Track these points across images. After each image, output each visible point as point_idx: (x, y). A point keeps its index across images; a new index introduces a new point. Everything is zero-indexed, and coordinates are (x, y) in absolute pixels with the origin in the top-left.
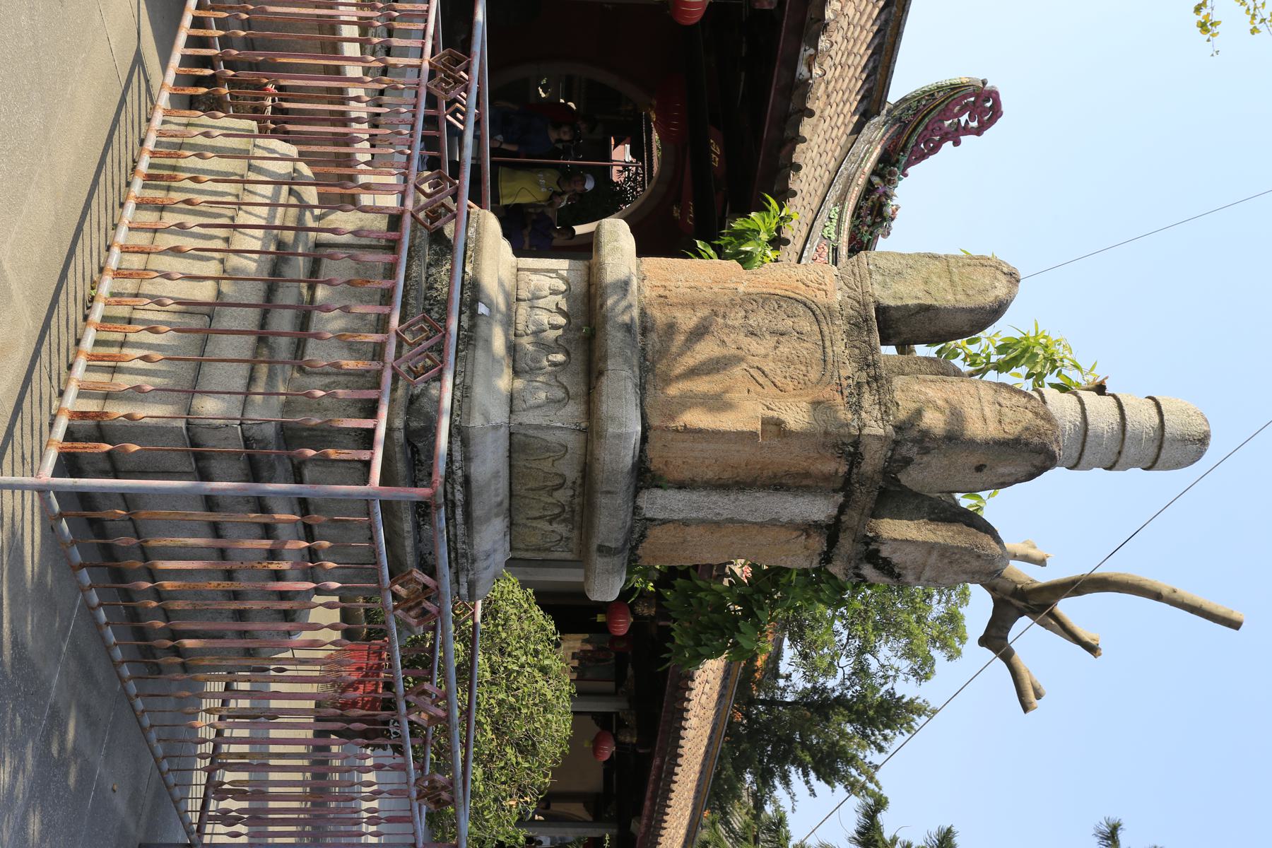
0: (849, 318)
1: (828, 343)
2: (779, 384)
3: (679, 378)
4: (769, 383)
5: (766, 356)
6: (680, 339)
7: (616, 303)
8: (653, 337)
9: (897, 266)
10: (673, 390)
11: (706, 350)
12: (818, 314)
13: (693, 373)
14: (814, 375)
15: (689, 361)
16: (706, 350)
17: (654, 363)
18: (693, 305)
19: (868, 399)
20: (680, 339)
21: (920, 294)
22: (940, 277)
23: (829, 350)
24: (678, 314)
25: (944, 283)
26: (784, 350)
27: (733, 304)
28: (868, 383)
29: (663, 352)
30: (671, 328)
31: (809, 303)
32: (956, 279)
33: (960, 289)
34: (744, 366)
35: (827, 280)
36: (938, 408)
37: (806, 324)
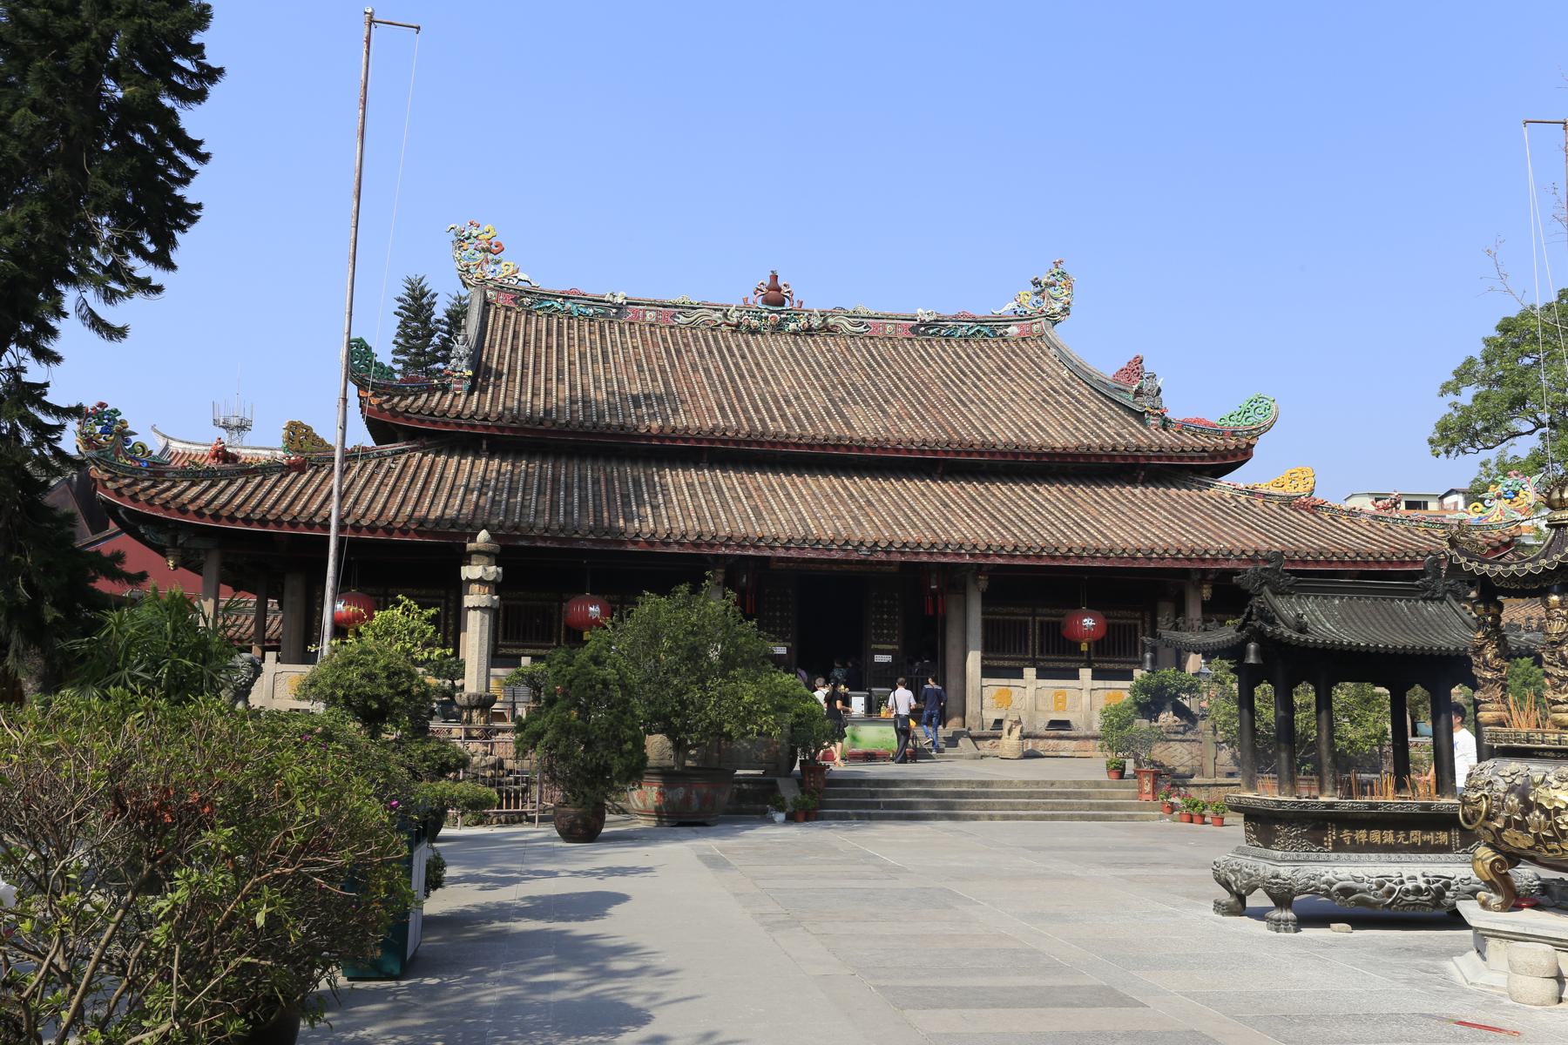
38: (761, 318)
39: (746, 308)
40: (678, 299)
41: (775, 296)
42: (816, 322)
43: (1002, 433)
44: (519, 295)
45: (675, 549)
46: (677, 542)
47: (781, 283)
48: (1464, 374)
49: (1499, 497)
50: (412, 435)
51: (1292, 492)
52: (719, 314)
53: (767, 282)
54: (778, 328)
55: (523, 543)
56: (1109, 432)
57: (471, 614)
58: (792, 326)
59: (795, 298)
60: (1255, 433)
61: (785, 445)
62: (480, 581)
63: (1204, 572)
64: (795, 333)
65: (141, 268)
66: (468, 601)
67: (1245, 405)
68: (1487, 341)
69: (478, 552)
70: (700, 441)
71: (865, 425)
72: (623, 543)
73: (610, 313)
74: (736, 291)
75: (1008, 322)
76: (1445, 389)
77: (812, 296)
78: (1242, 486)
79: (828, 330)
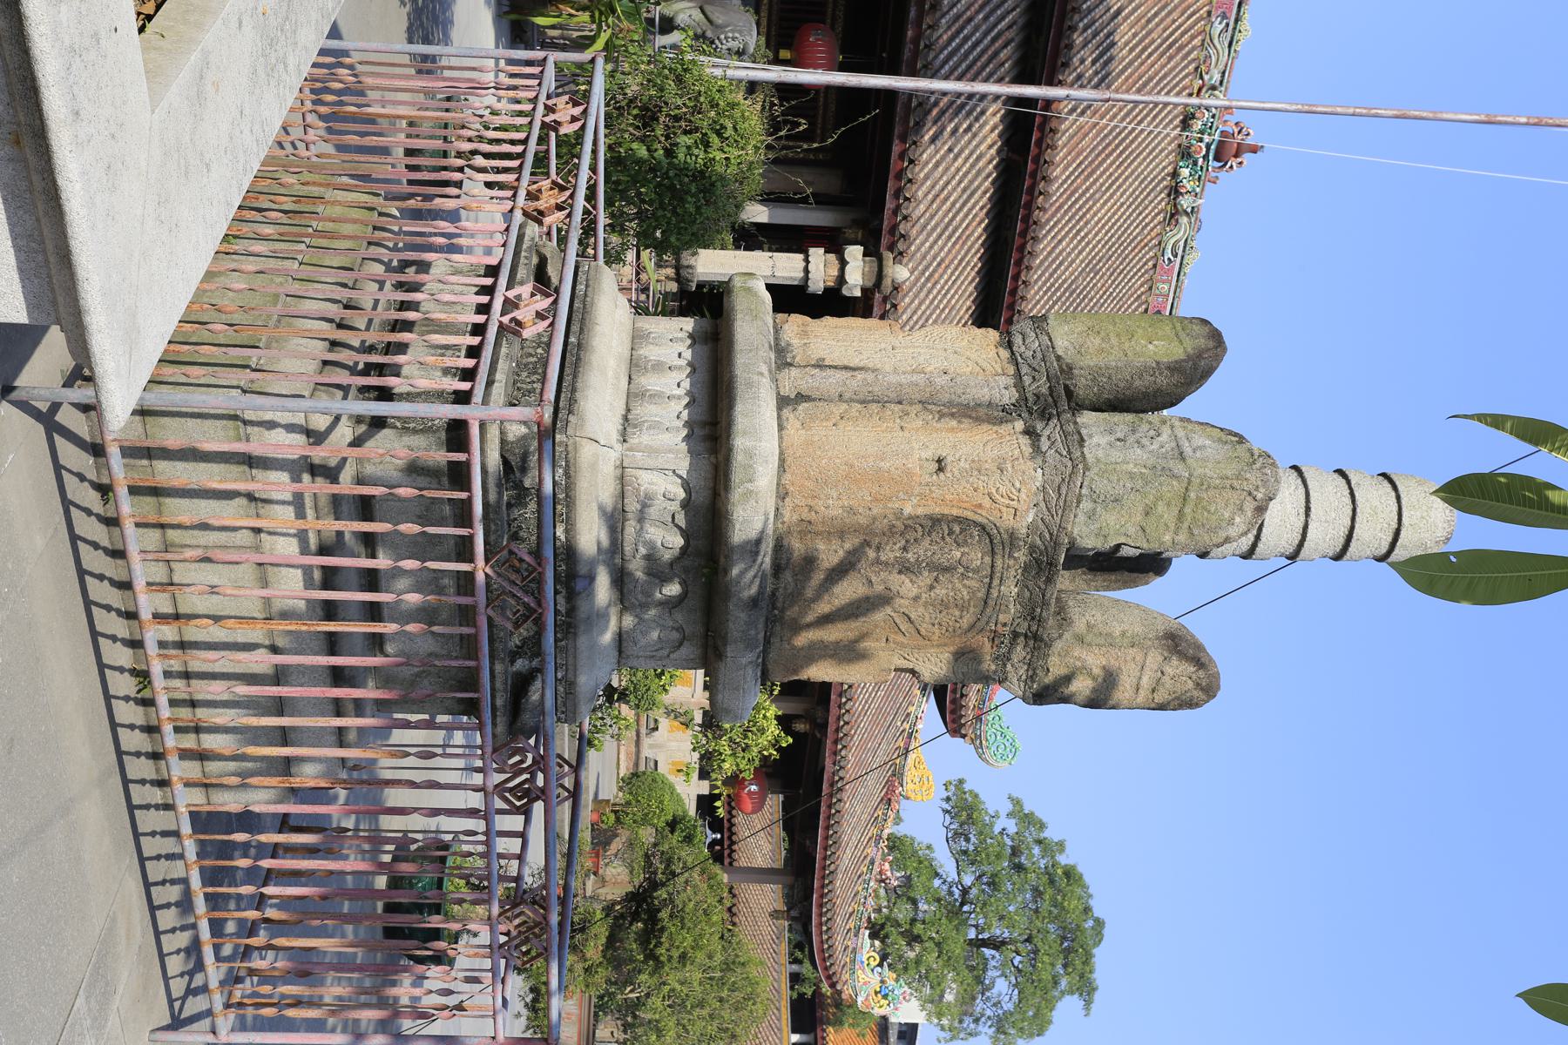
0: (1032, 549)
1: (996, 582)
2: (923, 632)
3: (809, 626)
4: (912, 630)
5: (916, 598)
6: (818, 577)
7: (742, 573)
8: (787, 576)
9: (1119, 491)
10: (802, 639)
11: (848, 590)
12: (996, 541)
13: (826, 620)
14: (966, 622)
15: (824, 608)
16: (848, 590)
17: (783, 610)
18: (841, 534)
19: (1020, 652)
20: (818, 577)
21: (1132, 530)
22: (1168, 505)
23: (995, 593)
24: (821, 546)
25: (1169, 516)
26: (940, 592)
27: (891, 531)
28: (1026, 636)
29: (796, 596)
30: (810, 561)
31: (989, 526)
32: (1187, 510)
33: (1186, 525)
34: (889, 610)
35: (1023, 496)
36: (1090, 674)
37: (976, 556)
38: (1202, 132)
40: (1245, 24)
42: (1185, 202)
45: (890, 205)
46: (898, 207)
47: (1247, 158)
48: (1028, 820)
49: (882, 982)
51: (908, 778)
52: (1217, 77)
53: (1249, 141)
54: (1185, 153)
55: (913, 14)
57: (798, 258)
58: (1185, 172)
59: (1222, 174)
60: (977, 742)
61: (1019, 263)
62: (841, 279)
63: (825, 725)
64: (1175, 174)
66: (817, 254)
67: (1009, 735)
68: (1061, 846)
69: (880, 276)
70: (1036, 160)
72: (903, 139)
76: (1017, 802)
77: (1221, 198)
78: (920, 726)
79: (1174, 215)
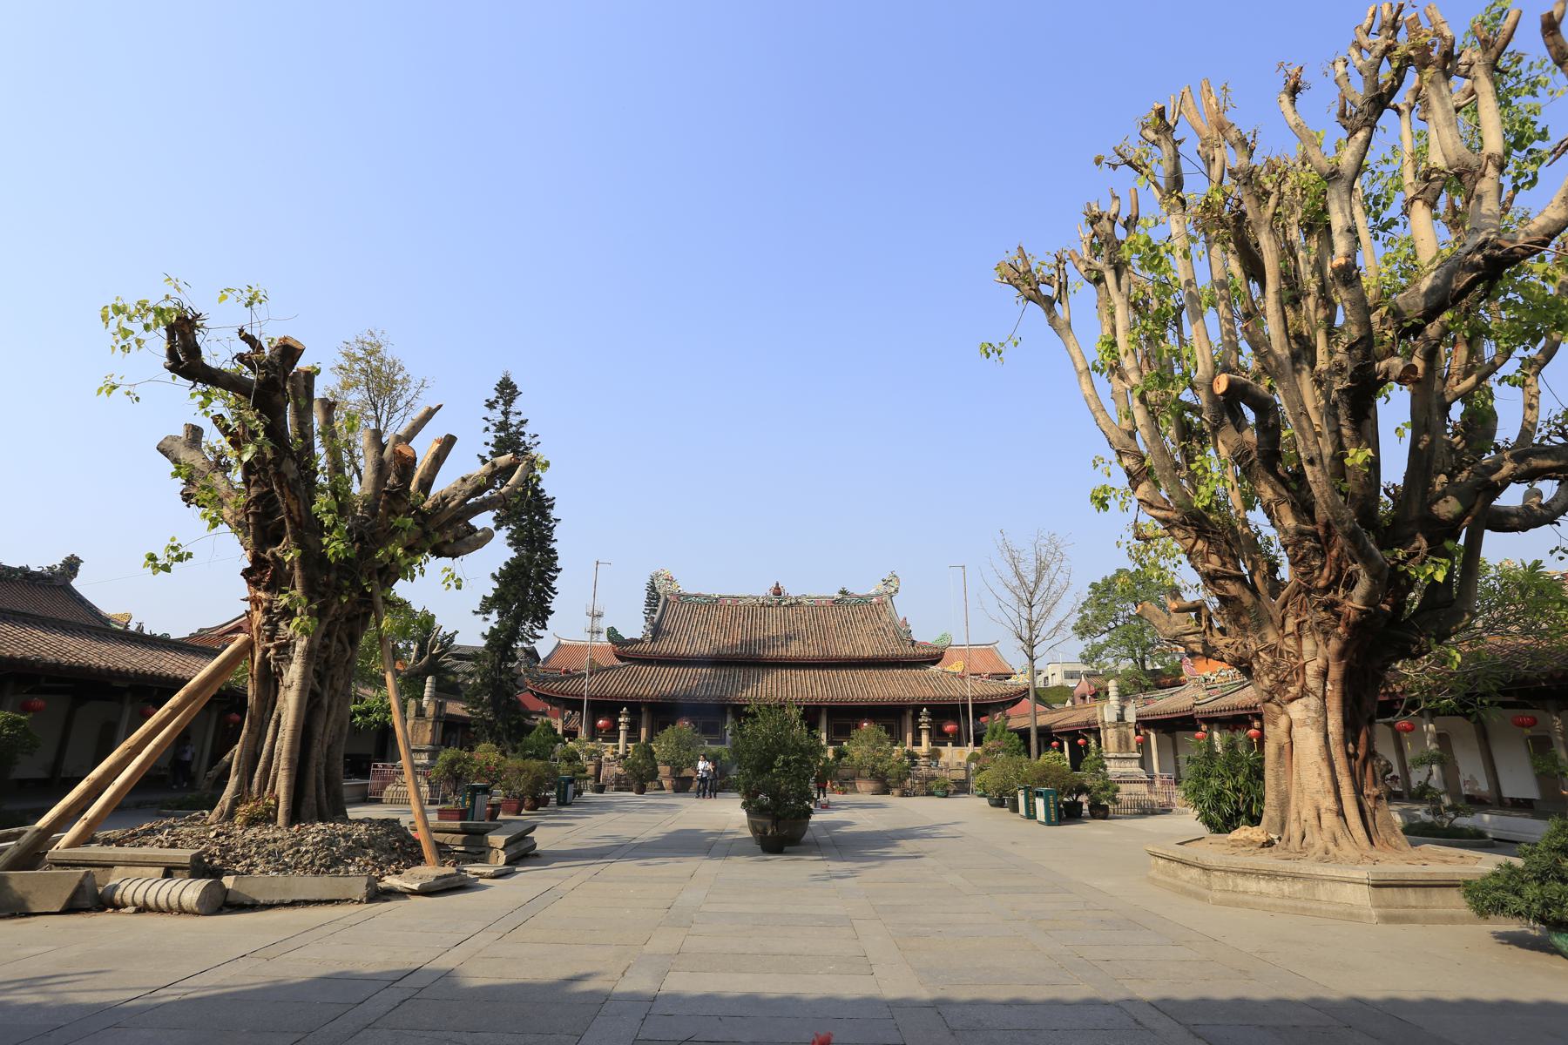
39: (767, 597)
41: (778, 591)
43: (846, 651)
44: (679, 595)
50: (630, 659)
56: (893, 649)
65: (538, 632)
71: (795, 650)
73: (713, 603)
74: (763, 590)
75: (872, 597)
77: (792, 590)
